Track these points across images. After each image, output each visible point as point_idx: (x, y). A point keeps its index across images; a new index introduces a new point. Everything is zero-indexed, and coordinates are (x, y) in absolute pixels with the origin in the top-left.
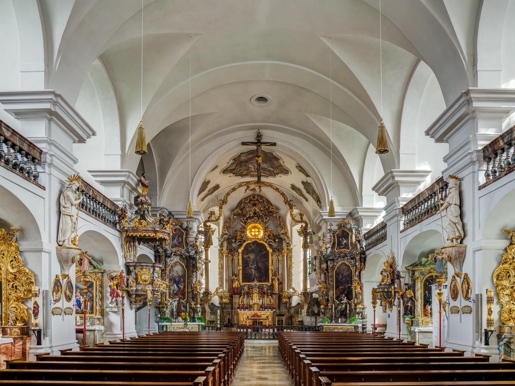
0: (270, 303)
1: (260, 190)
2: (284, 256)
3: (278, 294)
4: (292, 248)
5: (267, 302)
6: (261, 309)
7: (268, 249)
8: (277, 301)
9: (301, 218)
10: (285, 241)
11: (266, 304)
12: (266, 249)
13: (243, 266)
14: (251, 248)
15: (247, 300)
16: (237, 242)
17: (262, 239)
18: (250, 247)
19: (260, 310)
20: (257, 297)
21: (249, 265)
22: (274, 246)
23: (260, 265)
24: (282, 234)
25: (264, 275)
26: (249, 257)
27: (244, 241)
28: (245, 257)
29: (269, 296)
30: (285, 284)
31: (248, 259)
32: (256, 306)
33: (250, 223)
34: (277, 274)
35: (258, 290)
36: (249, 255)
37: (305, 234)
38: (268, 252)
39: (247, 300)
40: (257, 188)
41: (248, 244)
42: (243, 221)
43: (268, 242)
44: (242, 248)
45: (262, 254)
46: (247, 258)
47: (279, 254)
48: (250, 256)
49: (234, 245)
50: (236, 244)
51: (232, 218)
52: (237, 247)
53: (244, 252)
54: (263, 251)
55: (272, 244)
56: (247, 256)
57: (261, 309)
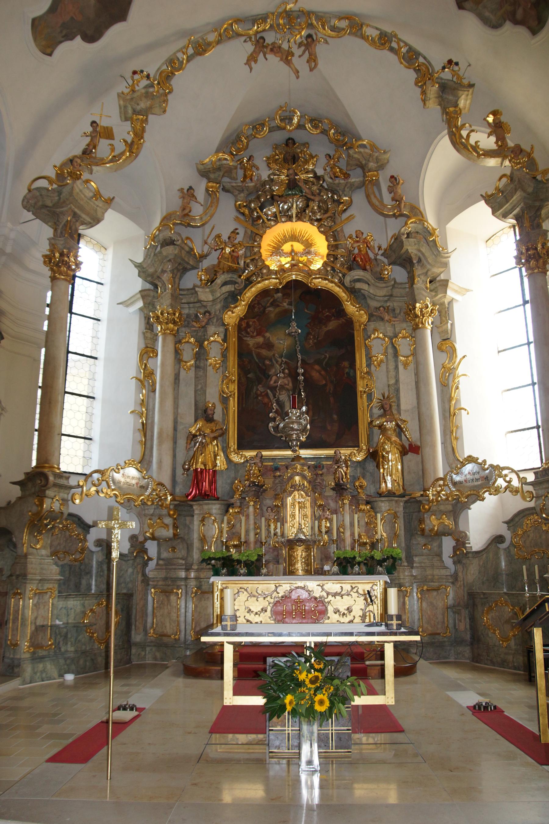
0: (365, 540)
1: (310, 54)
2: (424, 327)
3: (402, 496)
4: (451, 302)
5: (352, 534)
6: (326, 568)
7: (351, 308)
8: (400, 526)
9: (501, 139)
10: (423, 266)
11: (348, 541)
12: (341, 312)
13: (243, 380)
14: (278, 310)
15: (257, 527)
16: (219, 281)
17: (323, 273)
18: (272, 304)
19: (320, 572)
20: (302, 506)
21: (269, 377)
22: (374, 297)
23: (315, 375)
24: (409, 235)
25: (335, 417)
26: (269, 346)
27: (249, 282)
28: (251, 342)
29: (363, 507)
30: (433, 446)
31: (264, 352)
32: (300, 552)
33: (276, 219)
34: (395, 412)
35: (307, 474)
36: (268, 335)
37: (530, 190)
38: (349, 323)
39: (257, 527)
40: (297, 52)
41: (265, 293)
42: (247, 212)
43: (347, 280)
44: (240, 309)
45: (325, 329)
46: (259, 346)
47: (397, 330)
48: (274, 339)
49: (205, 295)
50: (212, 292)
51: (200, 194)
52: (218, 306)
53: (248, 326)
54: (328, 319)
55: (365, 287)
56: (260, 340)
57: (326, 568)
